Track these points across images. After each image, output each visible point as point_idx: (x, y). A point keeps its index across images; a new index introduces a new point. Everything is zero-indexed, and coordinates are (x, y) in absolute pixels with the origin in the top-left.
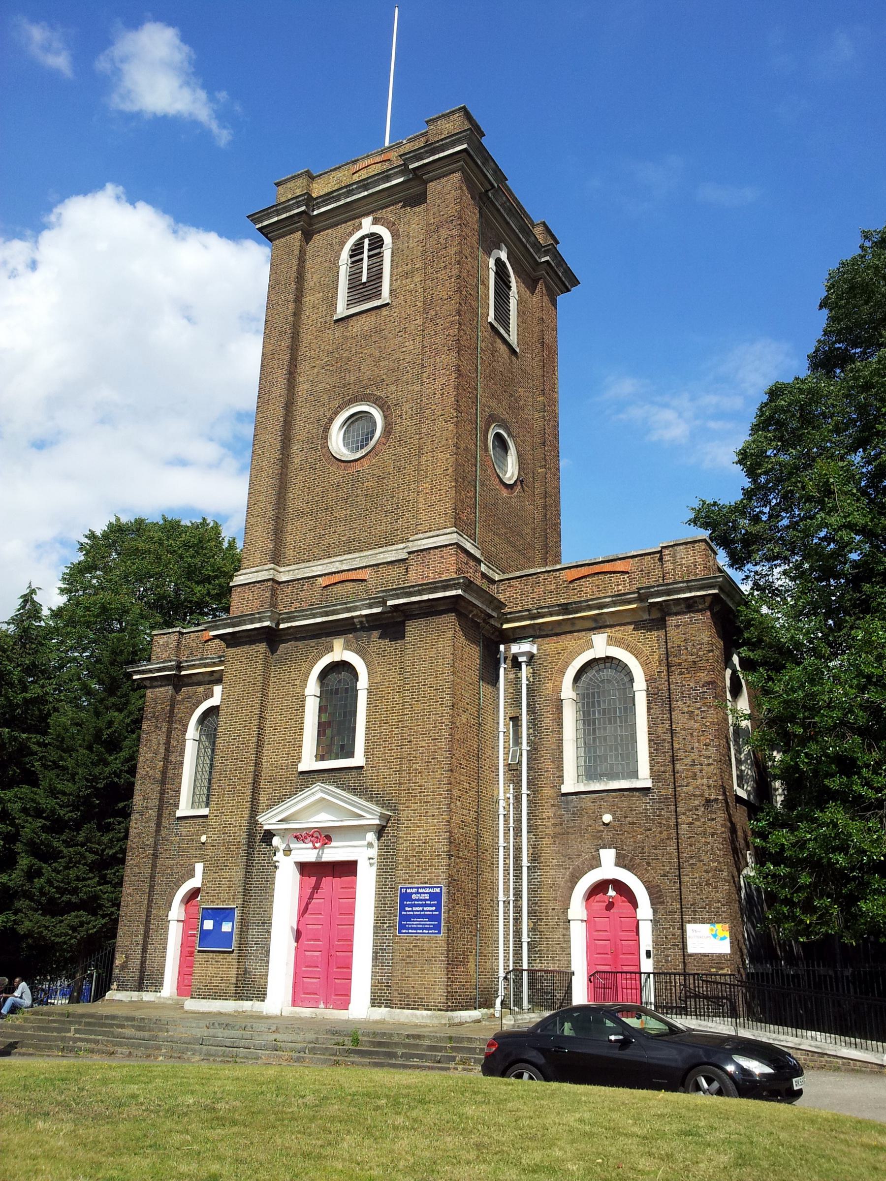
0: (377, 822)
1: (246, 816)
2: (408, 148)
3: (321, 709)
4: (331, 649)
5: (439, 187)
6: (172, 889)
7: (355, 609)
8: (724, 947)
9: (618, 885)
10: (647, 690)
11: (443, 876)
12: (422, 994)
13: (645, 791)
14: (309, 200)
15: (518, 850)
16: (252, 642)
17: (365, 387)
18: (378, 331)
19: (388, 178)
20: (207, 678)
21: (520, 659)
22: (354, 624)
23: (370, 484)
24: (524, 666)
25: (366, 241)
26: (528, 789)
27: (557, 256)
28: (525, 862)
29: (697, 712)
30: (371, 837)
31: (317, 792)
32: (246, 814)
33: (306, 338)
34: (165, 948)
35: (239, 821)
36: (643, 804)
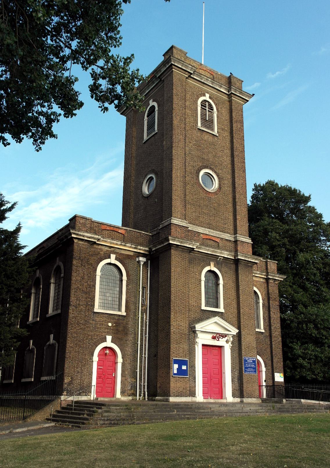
6: (92, 346)
13: (262, 333)
36: (262, 337)
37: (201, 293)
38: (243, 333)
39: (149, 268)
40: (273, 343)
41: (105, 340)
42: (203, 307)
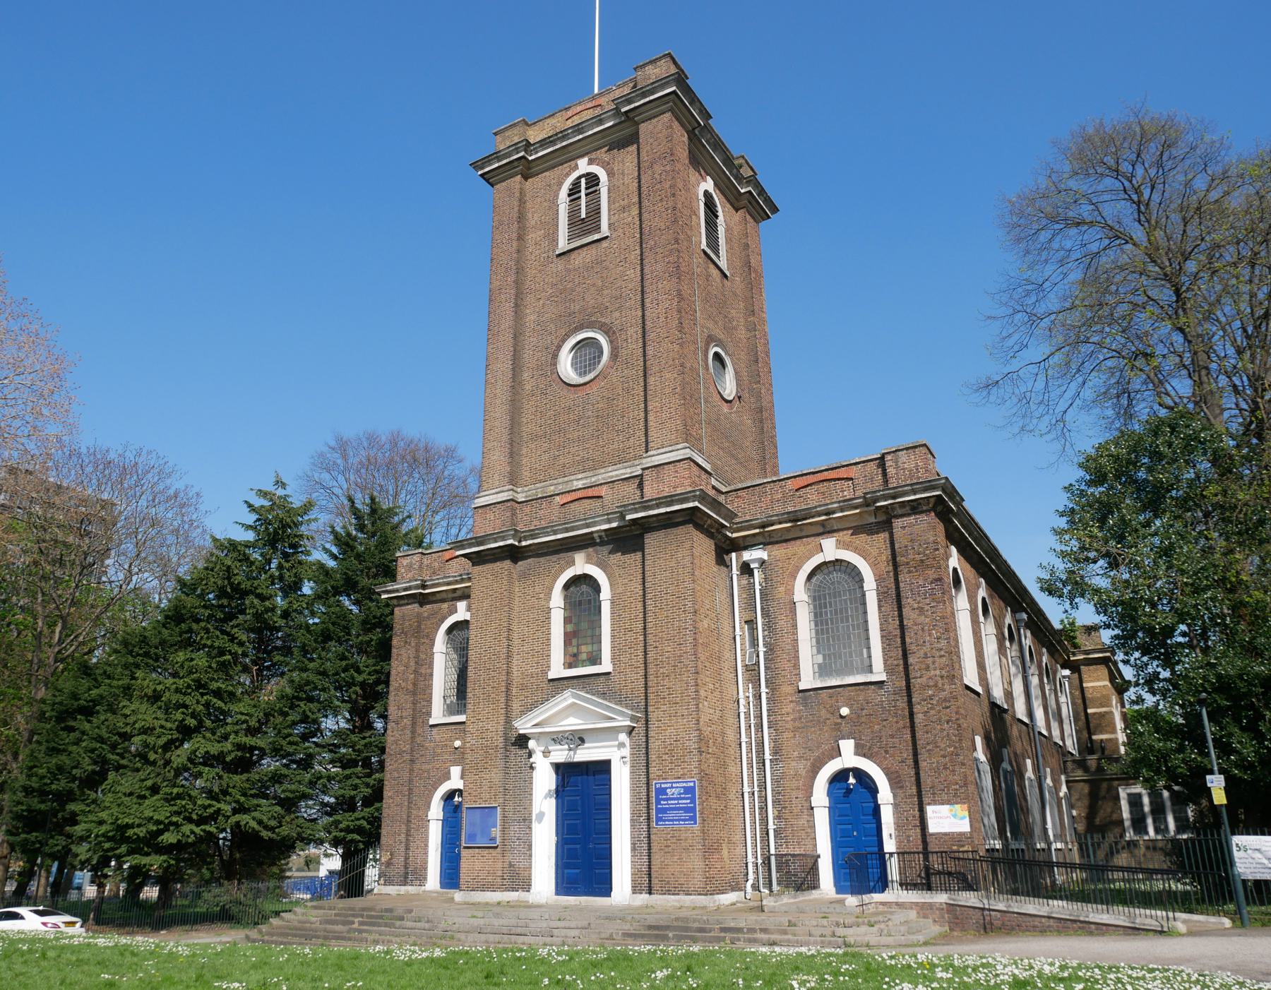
0: (628, 723)
1: (502, 722)
2: (618, 94)
3: (567, 620)
4: (572, 563)
5: (651, 127)
7: (594, 524)
8: (964, 826)
9: (859, 773)
10: (877, 590)
11: (696, 771)
12: (682, 880)
14: (528, 146)
15: (761, 744)
16: (495, 560)
17: (591, 315)
18: (599, 262)
19: (601, 122)
20: (450, 595)
21: (752, 566)
22: (593, 538)
23: (600, 406)
24: (756, 572)
25: (583, 181)
26: (767, 687)
27: (757, 185)
28: (768, 756)
29: (927, 607)
30: (623, 737)
31: (567, 698)
32: (502, 719)
33: (531, 272)
34: (427, 845)
35: (494, 727)
36: (880, 696)
40: (917, 708)
41: (447, 776)
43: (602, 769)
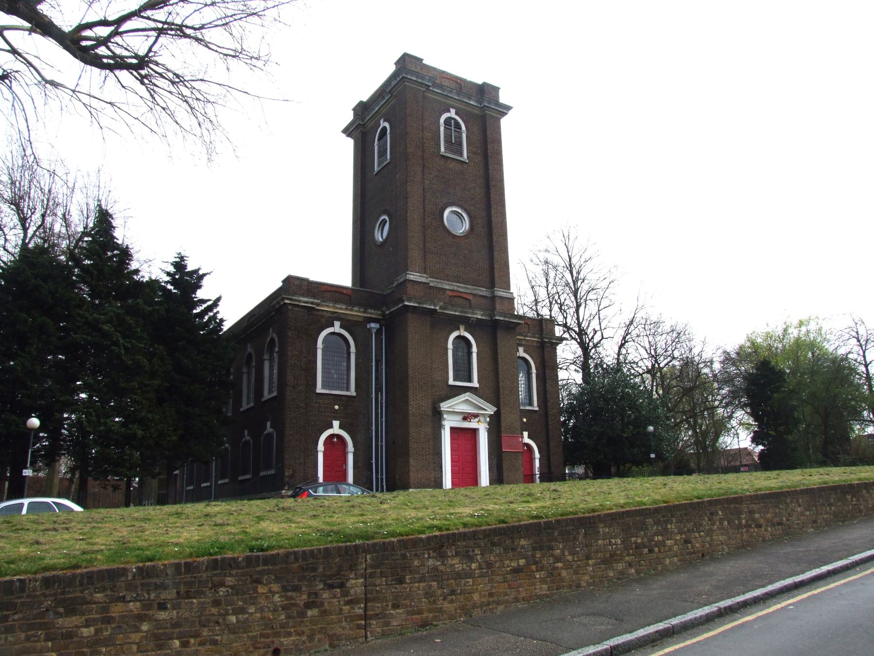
9: (527, 445)
31: (467, 396)
37: (447, 364)
38: (502, 412)
39: (384, 336)
42: (451, 382)
43: (475, 431)
